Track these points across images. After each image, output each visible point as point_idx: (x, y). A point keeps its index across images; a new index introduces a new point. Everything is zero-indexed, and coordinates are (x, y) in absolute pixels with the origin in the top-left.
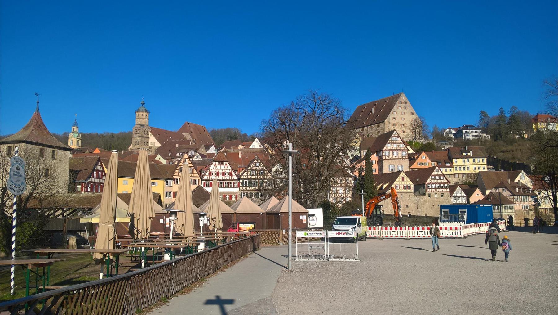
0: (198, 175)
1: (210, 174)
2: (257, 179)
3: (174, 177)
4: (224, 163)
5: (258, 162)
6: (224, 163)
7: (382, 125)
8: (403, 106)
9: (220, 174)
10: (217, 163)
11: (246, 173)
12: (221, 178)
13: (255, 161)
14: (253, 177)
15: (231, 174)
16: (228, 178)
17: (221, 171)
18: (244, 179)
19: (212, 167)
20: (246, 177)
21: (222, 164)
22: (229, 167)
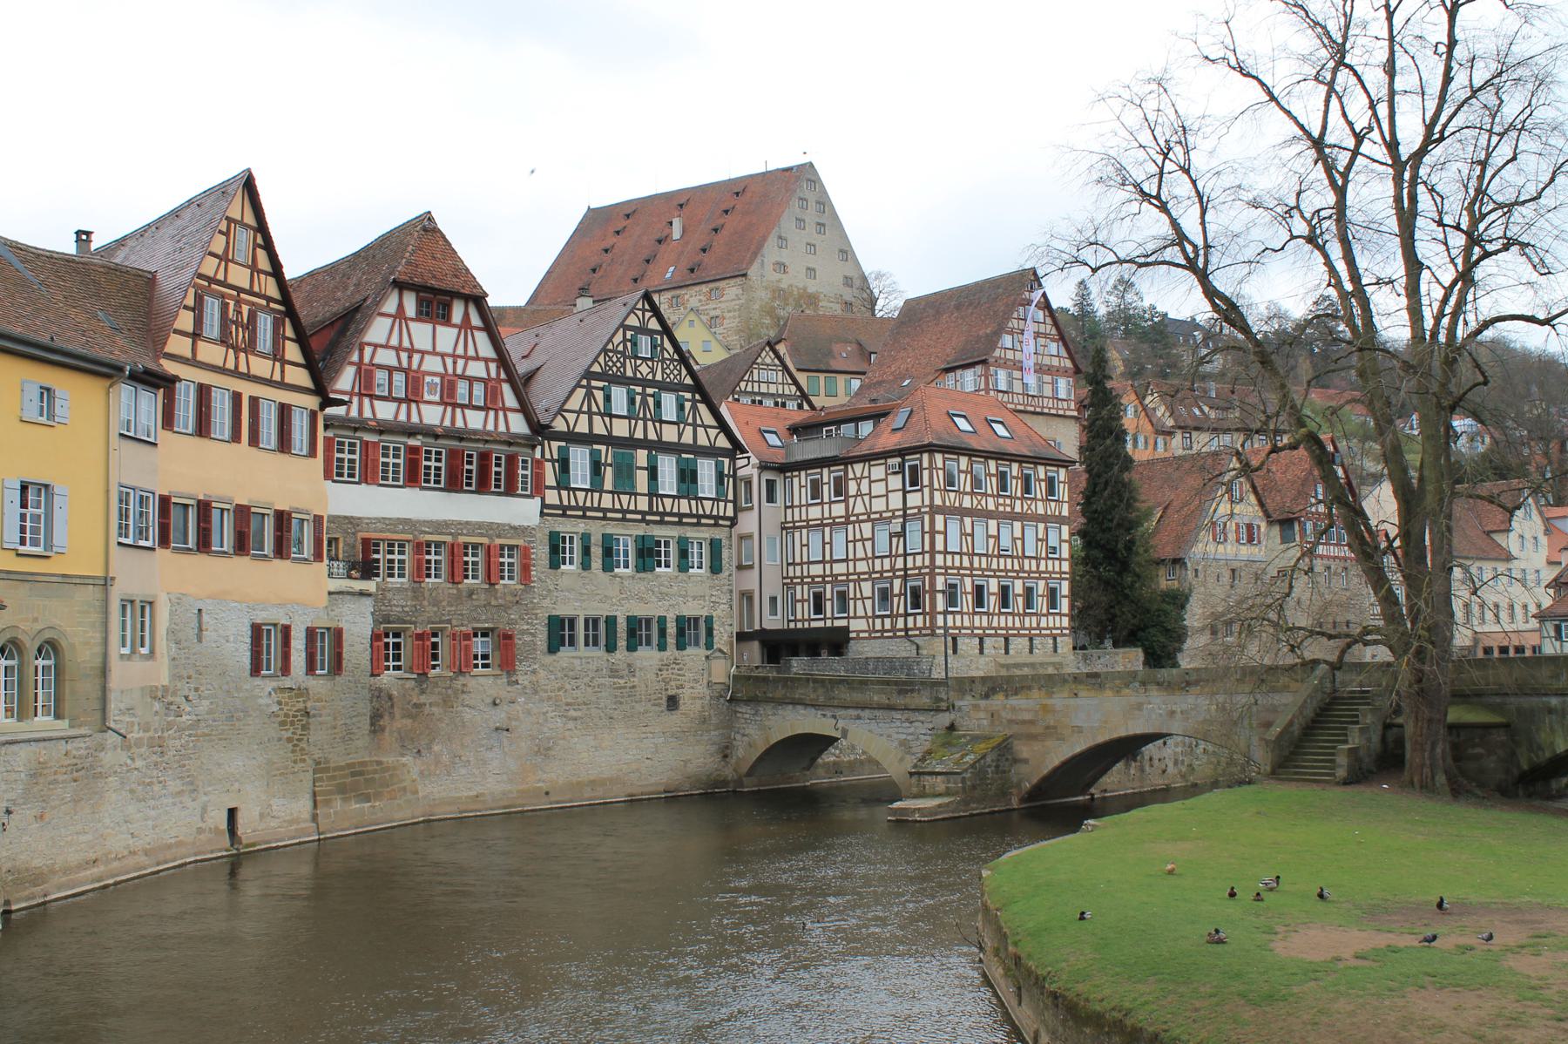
0: (301, 377)
1: (365, 388)
3: (171, 368)
4: (457, 313)
5: (643, 330)
12: (432, 415)
16: (475, 420)
17: (432, 364)
18: (572, 437)
19: (378, 330)
20: (582, 427)
21: (446, 320)
22: (486, 350)
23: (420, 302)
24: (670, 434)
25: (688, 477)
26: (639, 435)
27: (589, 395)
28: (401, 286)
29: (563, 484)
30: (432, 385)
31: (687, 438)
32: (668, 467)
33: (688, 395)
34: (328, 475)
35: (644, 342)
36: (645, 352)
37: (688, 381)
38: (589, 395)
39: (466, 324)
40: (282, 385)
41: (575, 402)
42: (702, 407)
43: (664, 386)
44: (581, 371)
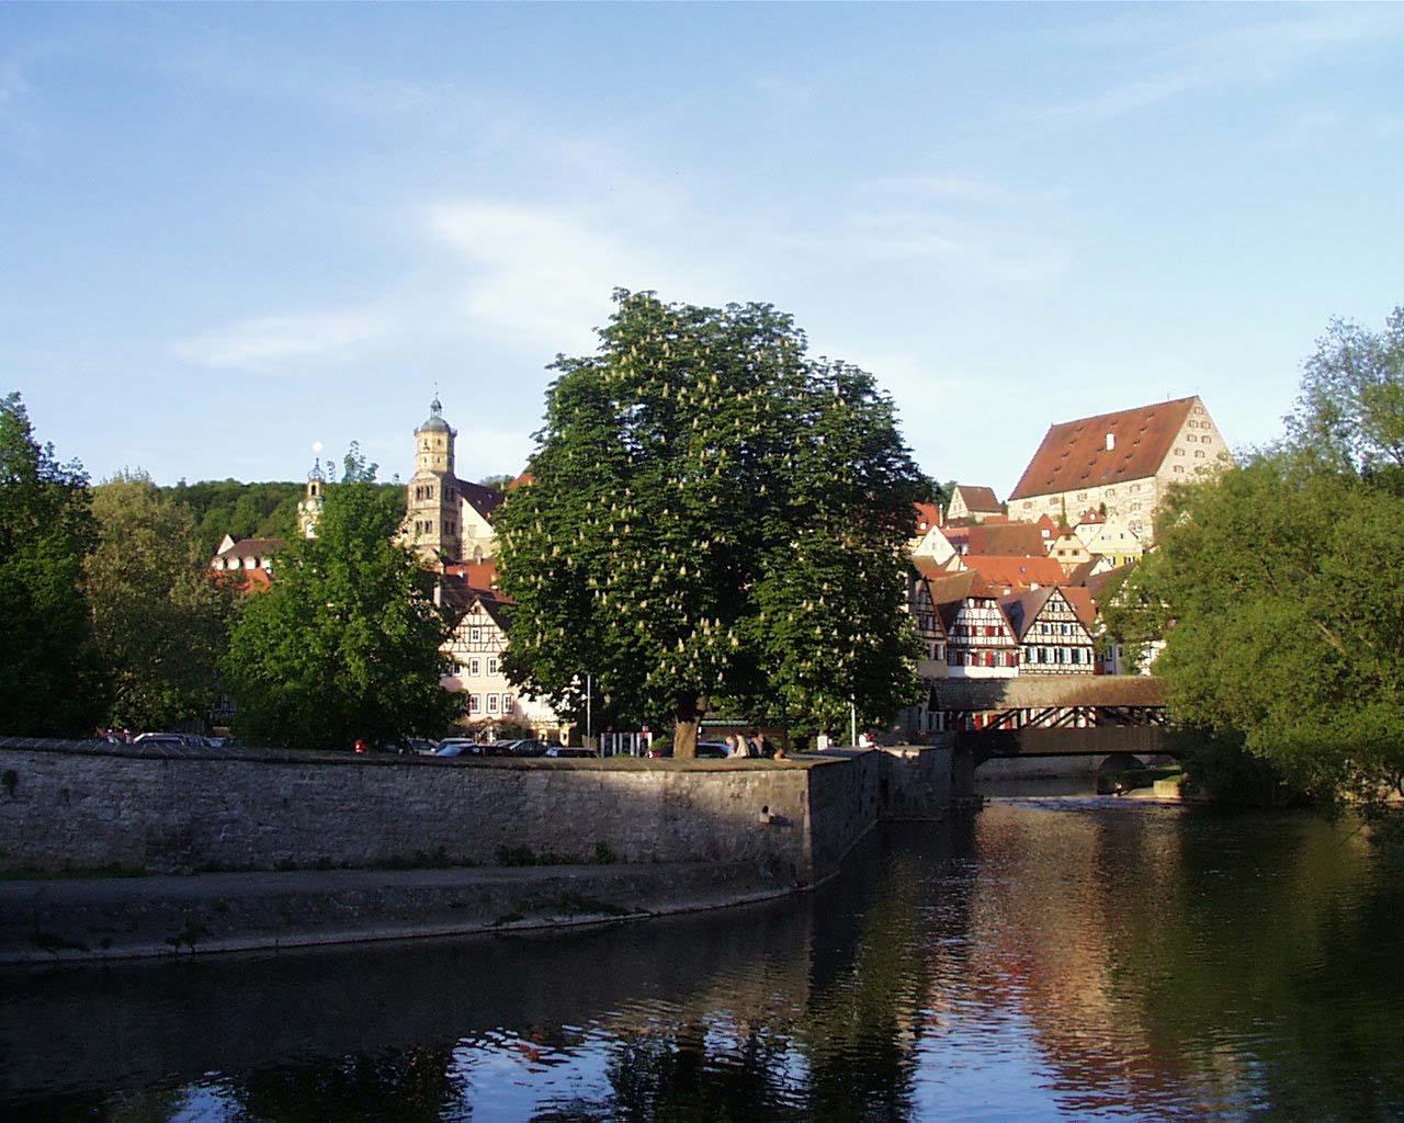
2: (1058, 644)
6: (988, 602)
7: (1146, 484)
8: (1199, 432)
9: (981, 631)
10: (971, 602)
11: (1033, 627)
12: (979, 640)
13: (1052, 598)
14: (1048, 640)
15: (1001, 633)
16: (994, 641)
17: (980, 623)
18: (1030, 644)
20: (1033, 641)
21: (982, 606)
22: (998, 615)
23: (975, 602)
24: (1067, 640)
25: (1075, 657)
26: (1055, 642)
27: (1035, 629)
28: (968, 598)
29: (1027, 660)
30: (981, 631)
31: (1074, 641)
32: (1067, 652)
33: (1074, 624)
34: (948, 664)
35: (1057, 605)
36: (1057, 609)
37: (1074, 619)
38: (1035, 629)
39: (991, 607)
40: (934, 638)
41: (1030, 632)
42: (1080, 629)
43: (1064, 622)
44: (1033, 617)
